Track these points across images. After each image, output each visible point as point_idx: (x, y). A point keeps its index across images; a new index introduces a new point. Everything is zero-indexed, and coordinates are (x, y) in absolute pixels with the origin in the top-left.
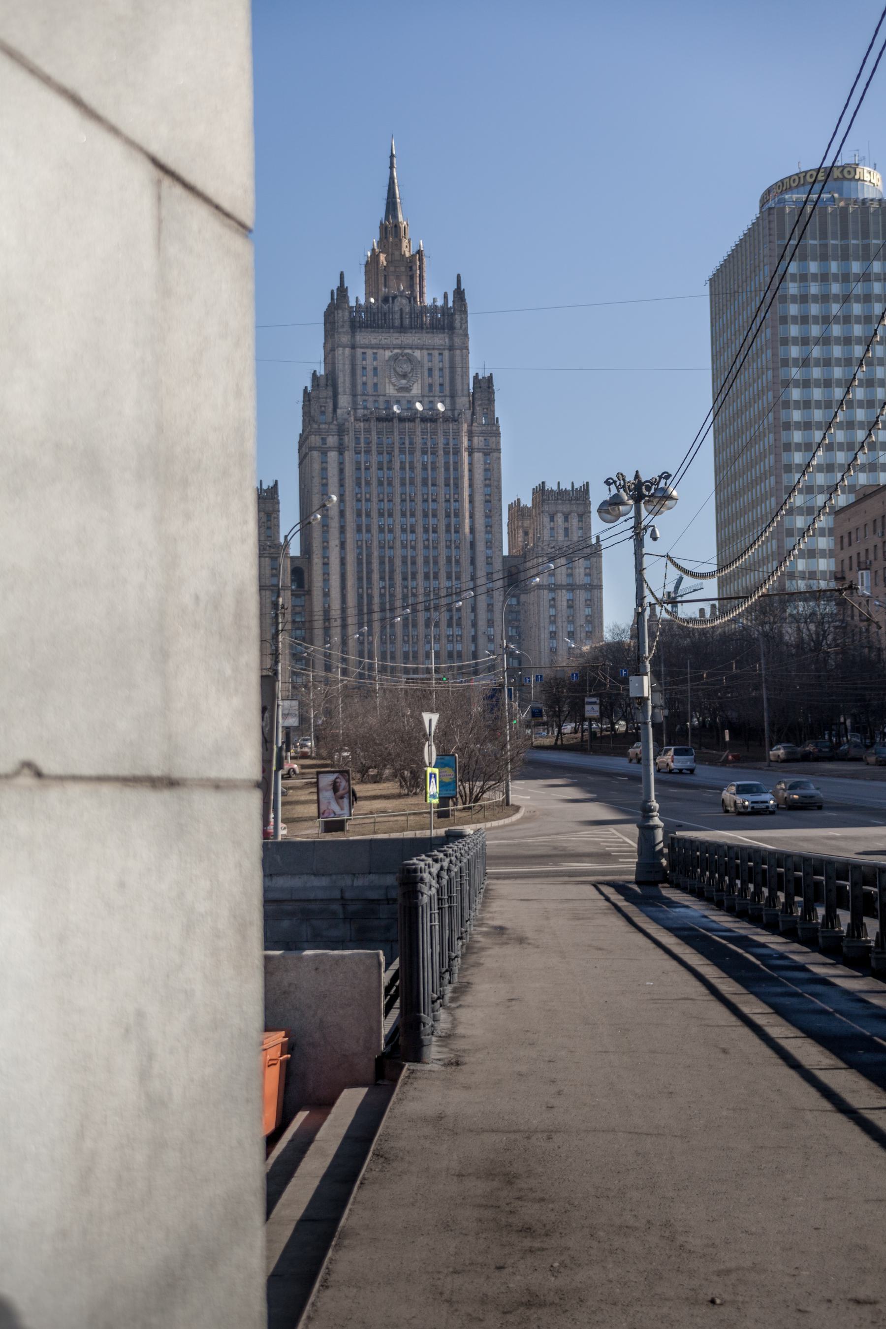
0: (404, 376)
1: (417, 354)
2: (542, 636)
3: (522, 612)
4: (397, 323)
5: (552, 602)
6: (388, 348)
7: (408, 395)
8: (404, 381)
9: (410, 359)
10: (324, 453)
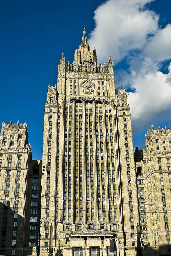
0: (88, 88)
1: (93, 81)
2: (158, 196)
3: (145, 188)
4: (85, 69)
5: (162, 179)
6: (81, 79)
7: (89, 95)
8: (87, 91)
9: (90, 83)
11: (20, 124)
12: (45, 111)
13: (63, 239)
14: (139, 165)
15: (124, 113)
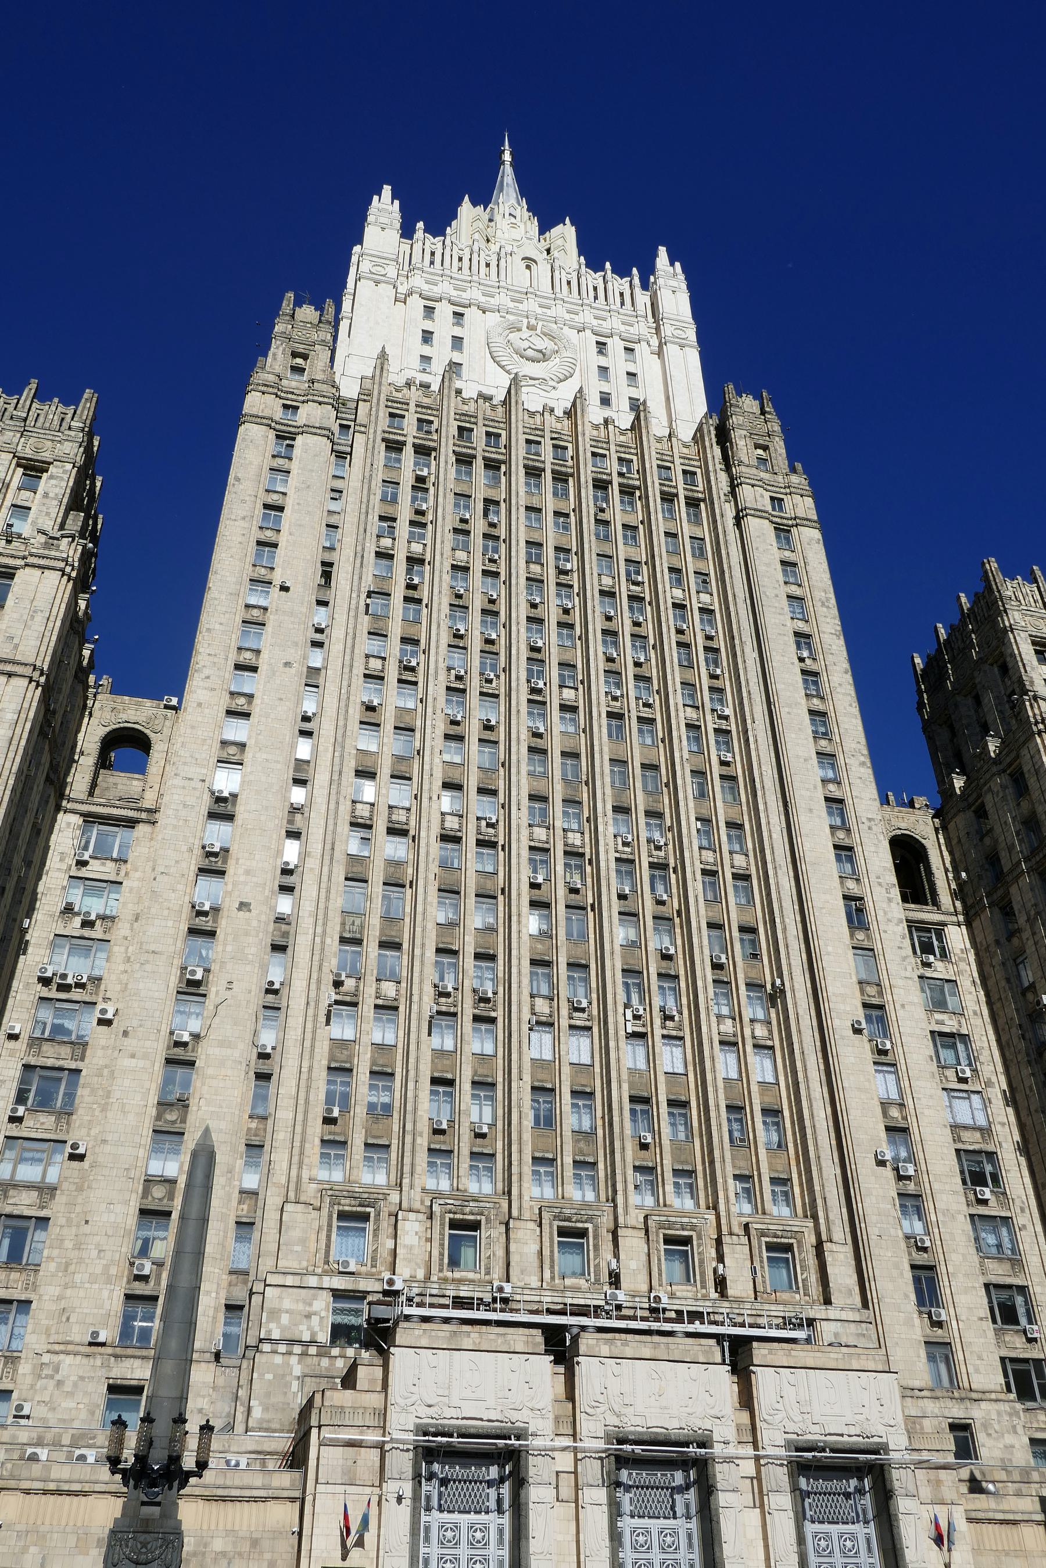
10: (286, 437)
11: (42, 396)
12: (247, 409)
13: (304, 1354)
14: (903, 825)
15: (777, 502)
